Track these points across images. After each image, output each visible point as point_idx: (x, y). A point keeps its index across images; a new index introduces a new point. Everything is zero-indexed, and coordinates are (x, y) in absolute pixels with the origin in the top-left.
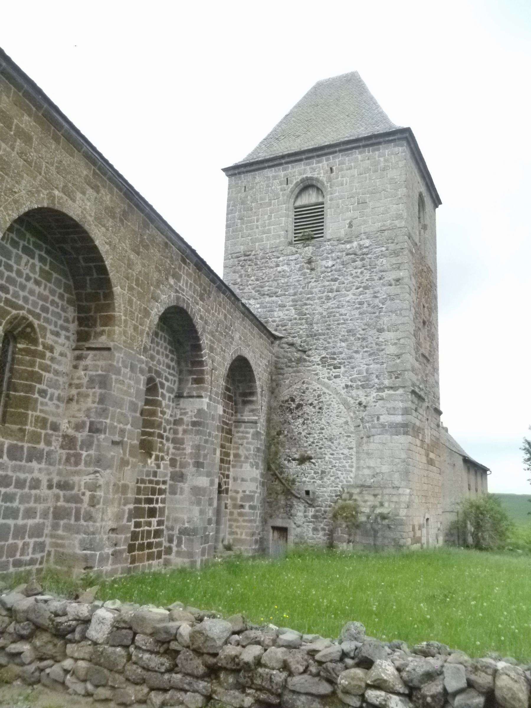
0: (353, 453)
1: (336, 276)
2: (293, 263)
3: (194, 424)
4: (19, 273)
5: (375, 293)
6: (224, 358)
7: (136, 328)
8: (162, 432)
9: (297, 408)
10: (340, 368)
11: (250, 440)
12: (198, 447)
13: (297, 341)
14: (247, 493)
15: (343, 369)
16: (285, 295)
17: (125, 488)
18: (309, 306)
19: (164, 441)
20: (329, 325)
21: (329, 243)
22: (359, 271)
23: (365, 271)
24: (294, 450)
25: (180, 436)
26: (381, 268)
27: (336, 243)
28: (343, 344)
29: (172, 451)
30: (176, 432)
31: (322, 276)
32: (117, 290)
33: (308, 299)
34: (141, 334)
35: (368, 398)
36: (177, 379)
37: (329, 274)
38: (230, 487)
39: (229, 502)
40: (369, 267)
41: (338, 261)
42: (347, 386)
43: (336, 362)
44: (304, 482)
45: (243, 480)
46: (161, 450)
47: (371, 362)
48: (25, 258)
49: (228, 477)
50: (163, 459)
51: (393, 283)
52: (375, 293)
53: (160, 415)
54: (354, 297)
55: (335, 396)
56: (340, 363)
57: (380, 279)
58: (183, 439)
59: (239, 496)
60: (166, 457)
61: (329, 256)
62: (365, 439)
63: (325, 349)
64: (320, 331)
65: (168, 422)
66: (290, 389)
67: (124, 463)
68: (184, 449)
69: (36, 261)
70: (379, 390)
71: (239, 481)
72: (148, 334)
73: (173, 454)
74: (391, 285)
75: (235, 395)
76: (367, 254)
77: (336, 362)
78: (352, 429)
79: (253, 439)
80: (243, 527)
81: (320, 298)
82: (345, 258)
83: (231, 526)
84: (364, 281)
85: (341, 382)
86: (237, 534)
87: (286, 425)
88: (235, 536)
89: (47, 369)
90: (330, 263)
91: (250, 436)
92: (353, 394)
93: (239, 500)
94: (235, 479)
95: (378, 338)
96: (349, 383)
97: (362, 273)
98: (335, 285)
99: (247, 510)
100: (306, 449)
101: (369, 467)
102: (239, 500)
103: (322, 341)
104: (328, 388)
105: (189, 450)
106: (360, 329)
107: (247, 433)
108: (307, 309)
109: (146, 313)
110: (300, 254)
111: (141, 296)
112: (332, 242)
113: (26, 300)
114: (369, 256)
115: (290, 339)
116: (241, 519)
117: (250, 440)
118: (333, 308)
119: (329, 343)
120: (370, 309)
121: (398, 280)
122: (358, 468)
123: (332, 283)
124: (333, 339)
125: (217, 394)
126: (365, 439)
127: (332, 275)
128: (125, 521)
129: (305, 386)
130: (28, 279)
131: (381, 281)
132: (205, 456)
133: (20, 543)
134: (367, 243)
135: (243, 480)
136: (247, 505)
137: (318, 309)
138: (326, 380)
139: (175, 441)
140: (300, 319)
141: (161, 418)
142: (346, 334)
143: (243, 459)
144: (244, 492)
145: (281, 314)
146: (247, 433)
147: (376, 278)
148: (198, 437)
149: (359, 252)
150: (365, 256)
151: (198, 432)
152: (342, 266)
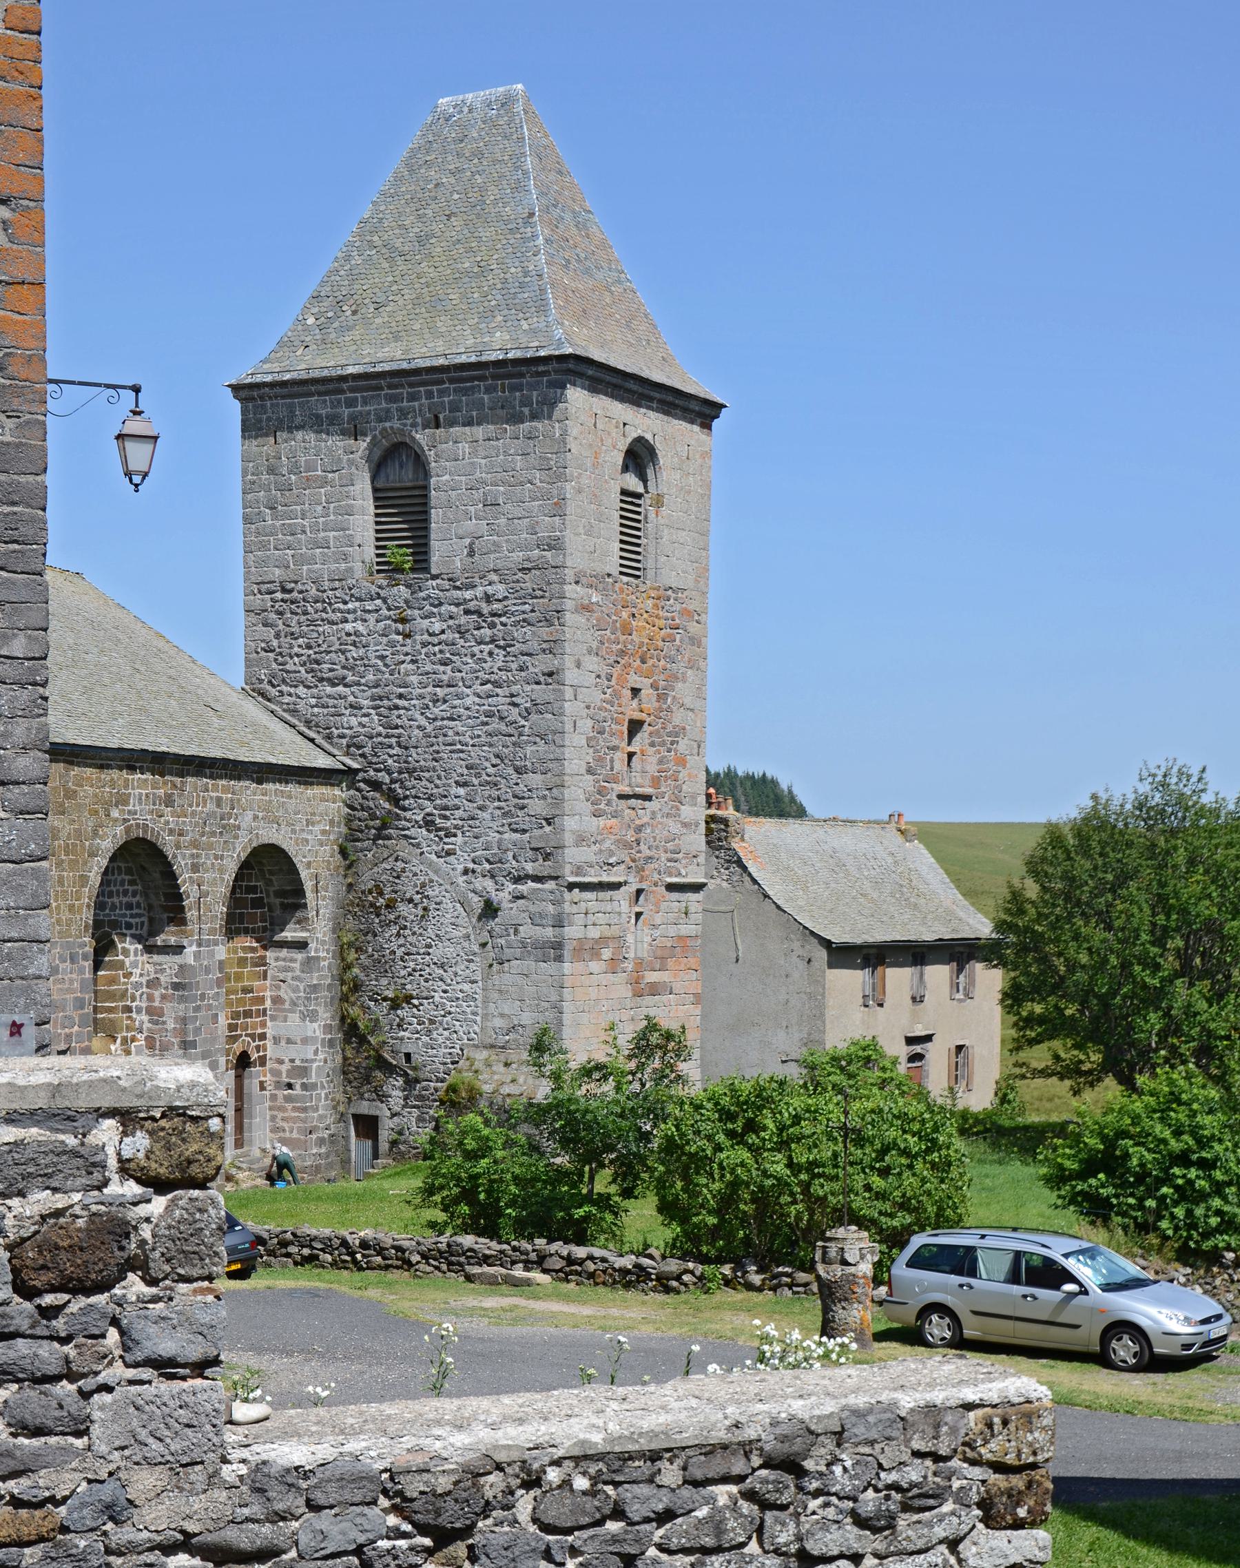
0: (478, 991)
1: (448, 655)
2: (372, 618)
3: (176, 986)
5: (512, 696)
6: (222, 870)
8: (128, 1003)
9: (387, 906)
10: (455, 836)
11: (298, 973)
12: (184, 1021)
13: (384, 777)
14: (298, 1063)
15: (459, 839)
16: (359, 684)
18: (402, 712)
19: (134, 1015)
20: (438, 752)
21: (434, 583)
22: (487, 648)
23: (496, 651)
24: (384, 981)
25: (157, 1004)
26: (524, 648)
27: (446, 585)
28: (461, 791)
29: (146, 1025)
30: (150, 998)
31: (423, 651)
33: (401, 696)
35: (501, 894)
36: (145, 919)
37: (437, 649)
38: (269, 1054)
39: (268, 1078)
40: (502, 643)
41: (451, 622)
42: (466, 872)
43: (449, 824)
44: (402, 1039)
45: (289, 1041)
46: (129, 1029)
47: (506, 827)
49: (263, 1037)
50: (133, 1039)
51: (542, 679)
52: (512, 696)
53: (122, 980)
54: (477, 700)
55: (448, 887)
56: (456, 827)
57: (521, 669)
58: (162, 1008)
59: (284, 1068)
60: (139, 1036)
61: (435, 610)
62: (496, 967)
63: (430, 798)
64: (422, 763)
65: (137, 986)
66: (376, 870)
68: (164, 1023)
70: (517, 880)
71: (283, 1043)
72: (88, 906)
73: (149, 1030)
74: (538, 683)
75: (268, 896)
76: (500, 616)
77: (449, 824)
78: (476, 948)
79: (303, 972)
80: (295, 1120)
81: (422, 697)
82: (463, 620)
83: (273, 1118)
84: (495, 670)
85: (461, 862)
86: (284, 1130)
87: (370, 937)
88: (281, 1134)
90: (437, 627)
91: (297, 965)
92: (477, 885)
93: (284, 1075)
94: (276, 1040)
95: (517, 784)
96: (471, 866)
97: (491, 654)
98: (446, 674)
99: (298, 1091)
100: (403, 981)
101: (502, 1015)
102: (284, 1075)
103: (424, 783)
104: (436, 872)
105: (171, 1025)
106: (487, 764)
107: (295, 961)
108: (399, 717)
109: (84, 880)
110: (385, 600)
111: (73, 863)
112: (439, 581)
114: (503, 619)
115: (372, 773)
116: (289, 1106)
117: (298, 973)
118: (443, 719)
119: (437, 787)
120: (503, 727)
121: (550, 674)
122: (485, 1017)
123: (442, 668)
124: (444, 781)
125: (212, 931)
126: (496, 967)
127: (441, 652)
129: (400, 865)
131: (523, 674)
132: (197, 1031)
134: (500, 590)
135: (289, 1041)
136: (297, 1083)
137: (415, 722)
138: (433, 857)
139: (150, 1011)
140: (387, 736)
141: (125, 983)
142: (466, 772)
143: (287, 1006)
144: (292, 1061)
145: (354, 721)
146: (295, 961)
147: (514, 666)
148: (182, 1006)
149: (485, 609)
150: (496, 619)
151: (182, 999)
152: (457, 635)
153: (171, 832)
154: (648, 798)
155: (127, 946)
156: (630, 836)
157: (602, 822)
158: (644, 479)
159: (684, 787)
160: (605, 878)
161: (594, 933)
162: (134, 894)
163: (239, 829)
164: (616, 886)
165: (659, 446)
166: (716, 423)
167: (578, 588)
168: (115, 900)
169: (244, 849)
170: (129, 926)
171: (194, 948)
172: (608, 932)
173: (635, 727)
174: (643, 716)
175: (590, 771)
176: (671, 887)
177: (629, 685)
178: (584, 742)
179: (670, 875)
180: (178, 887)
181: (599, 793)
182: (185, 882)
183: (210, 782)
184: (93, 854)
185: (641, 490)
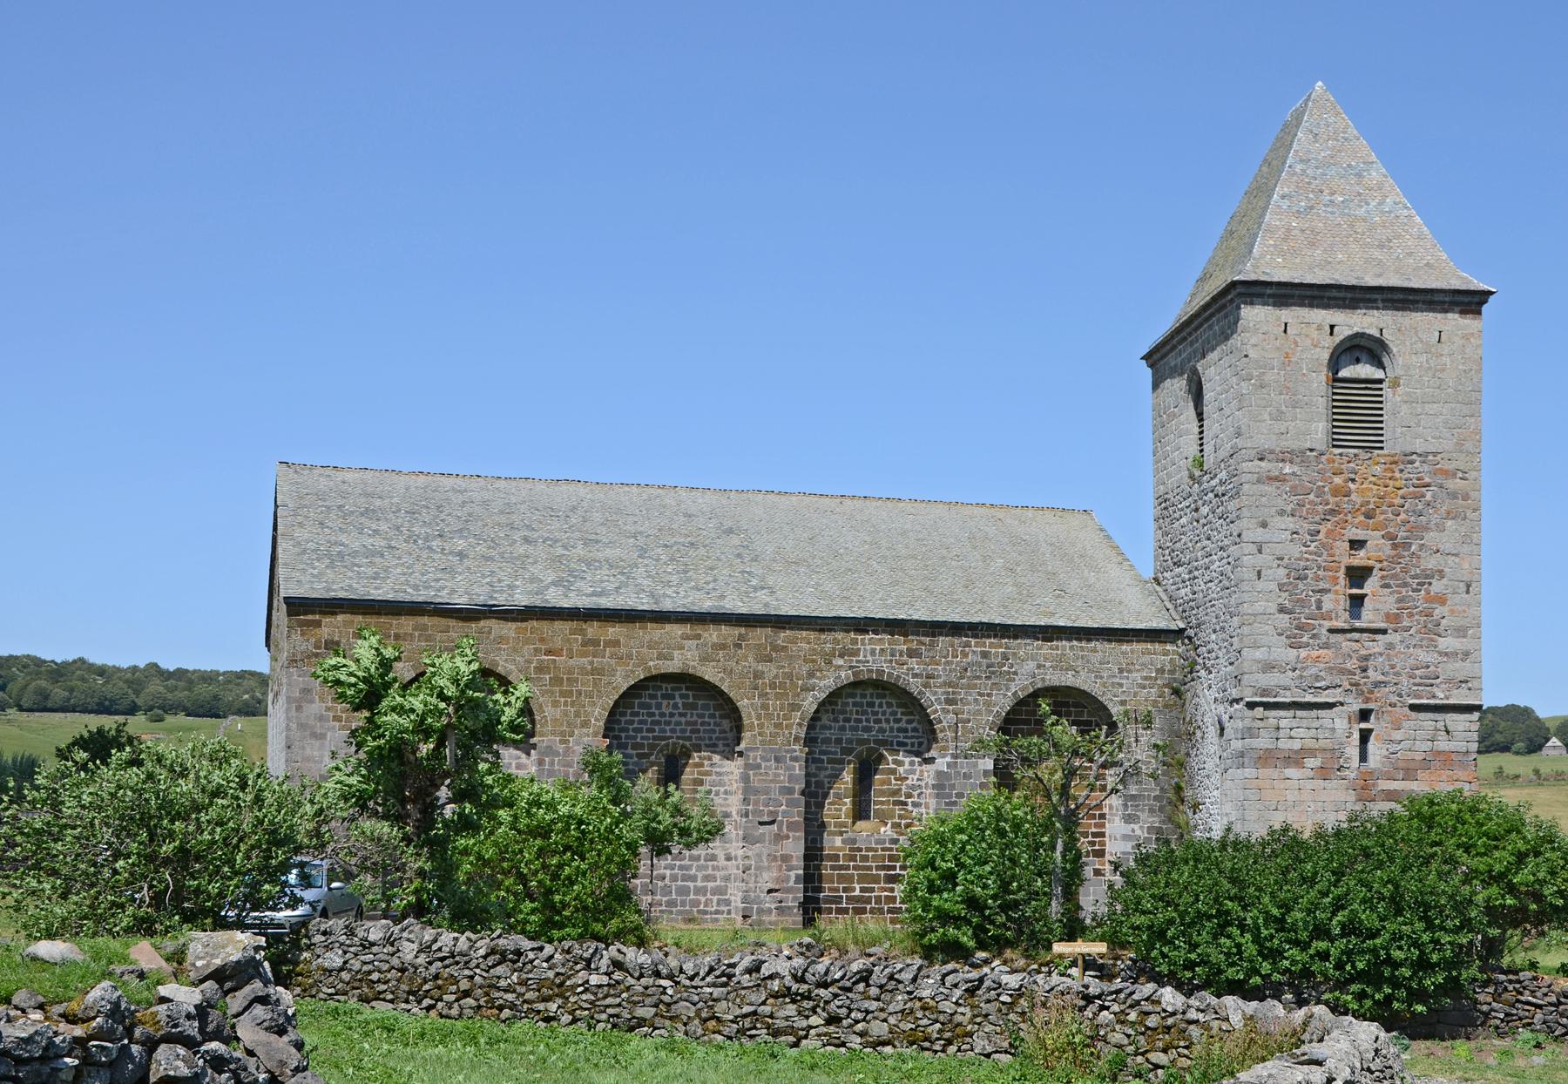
4: (662, 715)
7: (777, 726)
17: (786, 858)
32: (743, 704)
34: (789, 727)
48: (665, 702)
67: (779, 838)
69: (678, 700)
89: (708, 774)
113: (673, 731)
128: (791, 883)
130: (672, 715)
133: (703, 899)
153: (915, 676)
154: (1384, 632)
155: (900, 758)
156: (1352, 664)
157: (1303, 653)
158: (1381, 366)
159: (1444, 622)
160: (1309, 698)
161: (1297, 745)
162: (909, 722)
163: (1015, 673)
164: (1330, 706)
165: (1388, 336)
166: (1485, 308)
167: (1263, 464)
168: (884, 725)
169: (1022, 689)
170: (900, 744)
171: (948, 759)
172: (1311, 744)
173: (1358, 575)
174: (1371, 563)
175: (1282, 610)
176: (1413, 708)
177: (1346, 538)
178: (1273, 586)
179: (1416, 697)
180: (928, 715)
181: (1298, 628)
182: (936, 711)
183: (973, 641)
184: (806, 689)
185: (1379, 374)
